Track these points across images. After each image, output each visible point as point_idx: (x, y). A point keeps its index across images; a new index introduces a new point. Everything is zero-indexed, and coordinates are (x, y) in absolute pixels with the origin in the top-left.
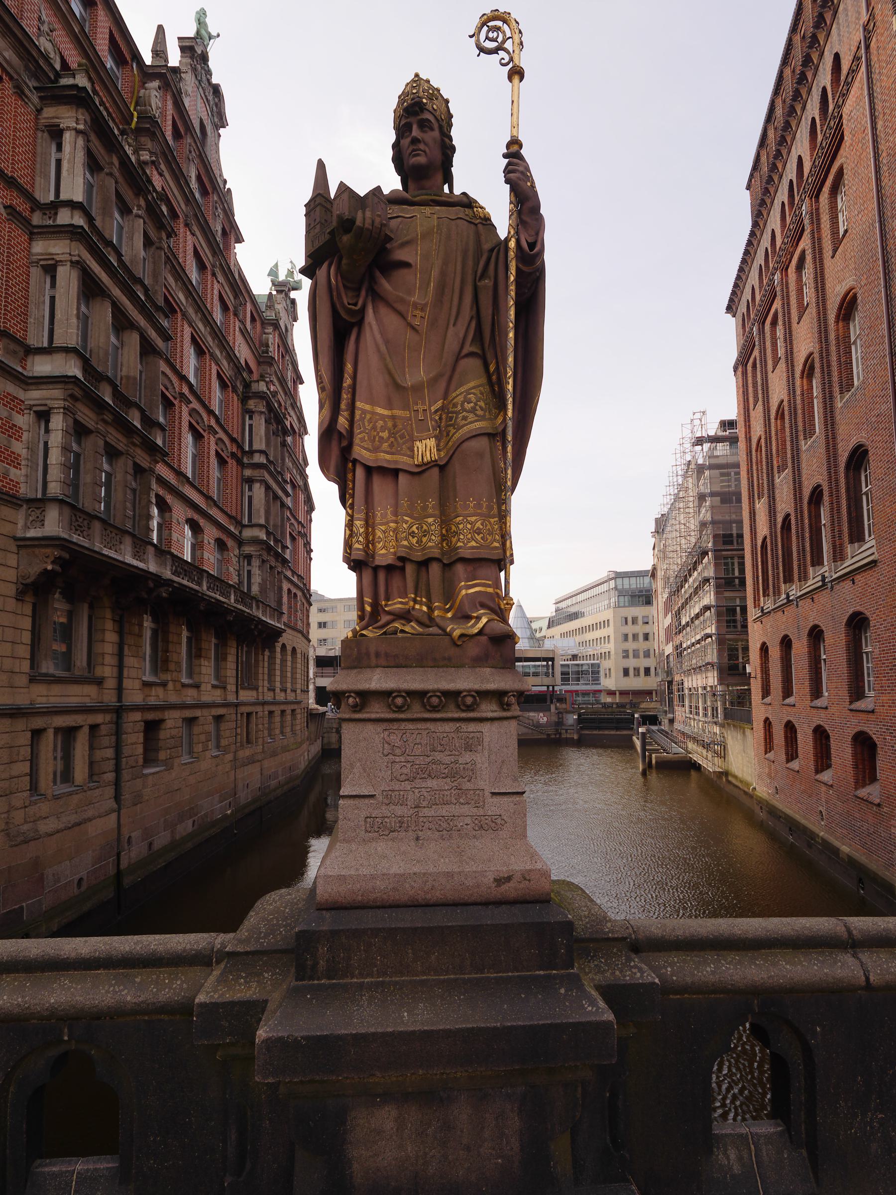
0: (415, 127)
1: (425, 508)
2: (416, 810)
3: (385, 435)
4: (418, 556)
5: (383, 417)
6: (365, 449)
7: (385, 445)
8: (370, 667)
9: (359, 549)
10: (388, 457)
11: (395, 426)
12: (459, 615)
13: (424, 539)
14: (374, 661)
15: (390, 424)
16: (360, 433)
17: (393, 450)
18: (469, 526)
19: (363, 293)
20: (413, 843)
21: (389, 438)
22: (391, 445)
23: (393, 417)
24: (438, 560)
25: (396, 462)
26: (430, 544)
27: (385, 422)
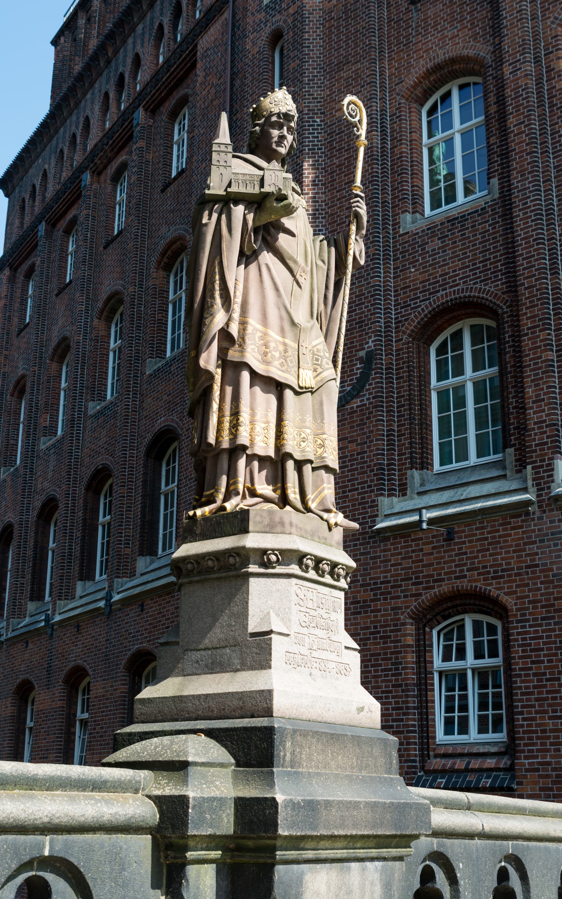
0: (285, 128)
1: (303, 421)
2: (310, 651)
3: (277, 354)
4: (298, 456)
5: (276, 341)
6: (256, 358)
7: (276, 363)
8: (284, 533)
9: (246, 437)
10: (280, 373)
11: (286, 351)
12: (321, 508)
13: (303, 444)
14: (288, 528)
15: (281, 348)
16: (252, 344)
17: (284, 369)
18: (331, 443)
19: (260, 238)
20: (309, 676)
21: (280, 358)
22: (282, 365)
23: (285, 344)
24: (311, 462)
25: (286, 379)
26: (308, 449)
27: (277, 345)
